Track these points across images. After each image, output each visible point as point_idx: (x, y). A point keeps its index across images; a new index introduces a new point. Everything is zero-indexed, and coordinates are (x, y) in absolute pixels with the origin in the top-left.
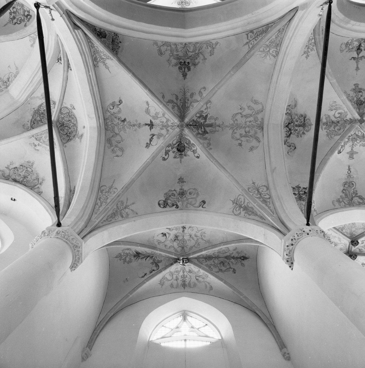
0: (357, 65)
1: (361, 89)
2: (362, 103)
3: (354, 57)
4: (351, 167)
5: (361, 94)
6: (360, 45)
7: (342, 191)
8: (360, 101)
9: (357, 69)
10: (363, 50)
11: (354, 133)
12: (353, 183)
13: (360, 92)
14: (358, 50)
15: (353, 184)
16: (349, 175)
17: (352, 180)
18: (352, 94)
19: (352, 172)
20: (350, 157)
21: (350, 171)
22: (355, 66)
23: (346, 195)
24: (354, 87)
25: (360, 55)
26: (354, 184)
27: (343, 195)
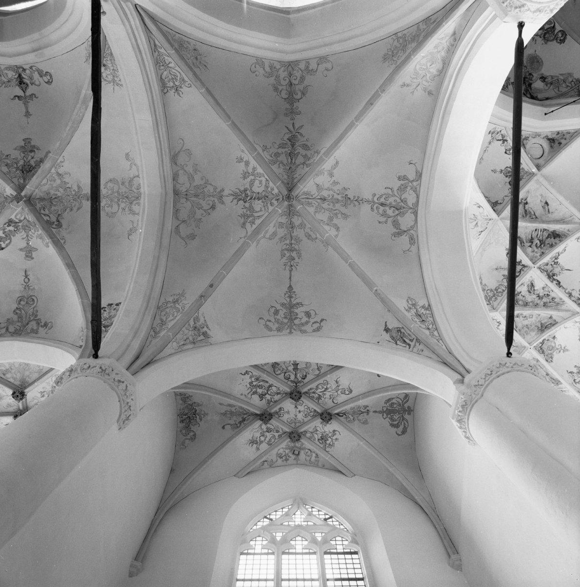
0: (27, 108)
1: (34, 146)
2: (31, 169)
3: (19, 95)
4: (28, 273)
5: (32, 154)
6: (20, 76)
7: (14, 311)
8: (29, 166)
9: (28, 114)
10: (30, 85)
11: (25, 218)
12: (33, 298)
13: (31, 151)
14: (21, 84)
15: (33, 300)
16: (27, 286)
17: (31, 294)
18: (17, 154)
19: (31, 280)
20: (27, 256)
21: (29, 279)
22: (24, 110)
23: (20, 317)
24: (23, 144)
25: (29, 92)
26: (35, 300)
27: (15, 318)
